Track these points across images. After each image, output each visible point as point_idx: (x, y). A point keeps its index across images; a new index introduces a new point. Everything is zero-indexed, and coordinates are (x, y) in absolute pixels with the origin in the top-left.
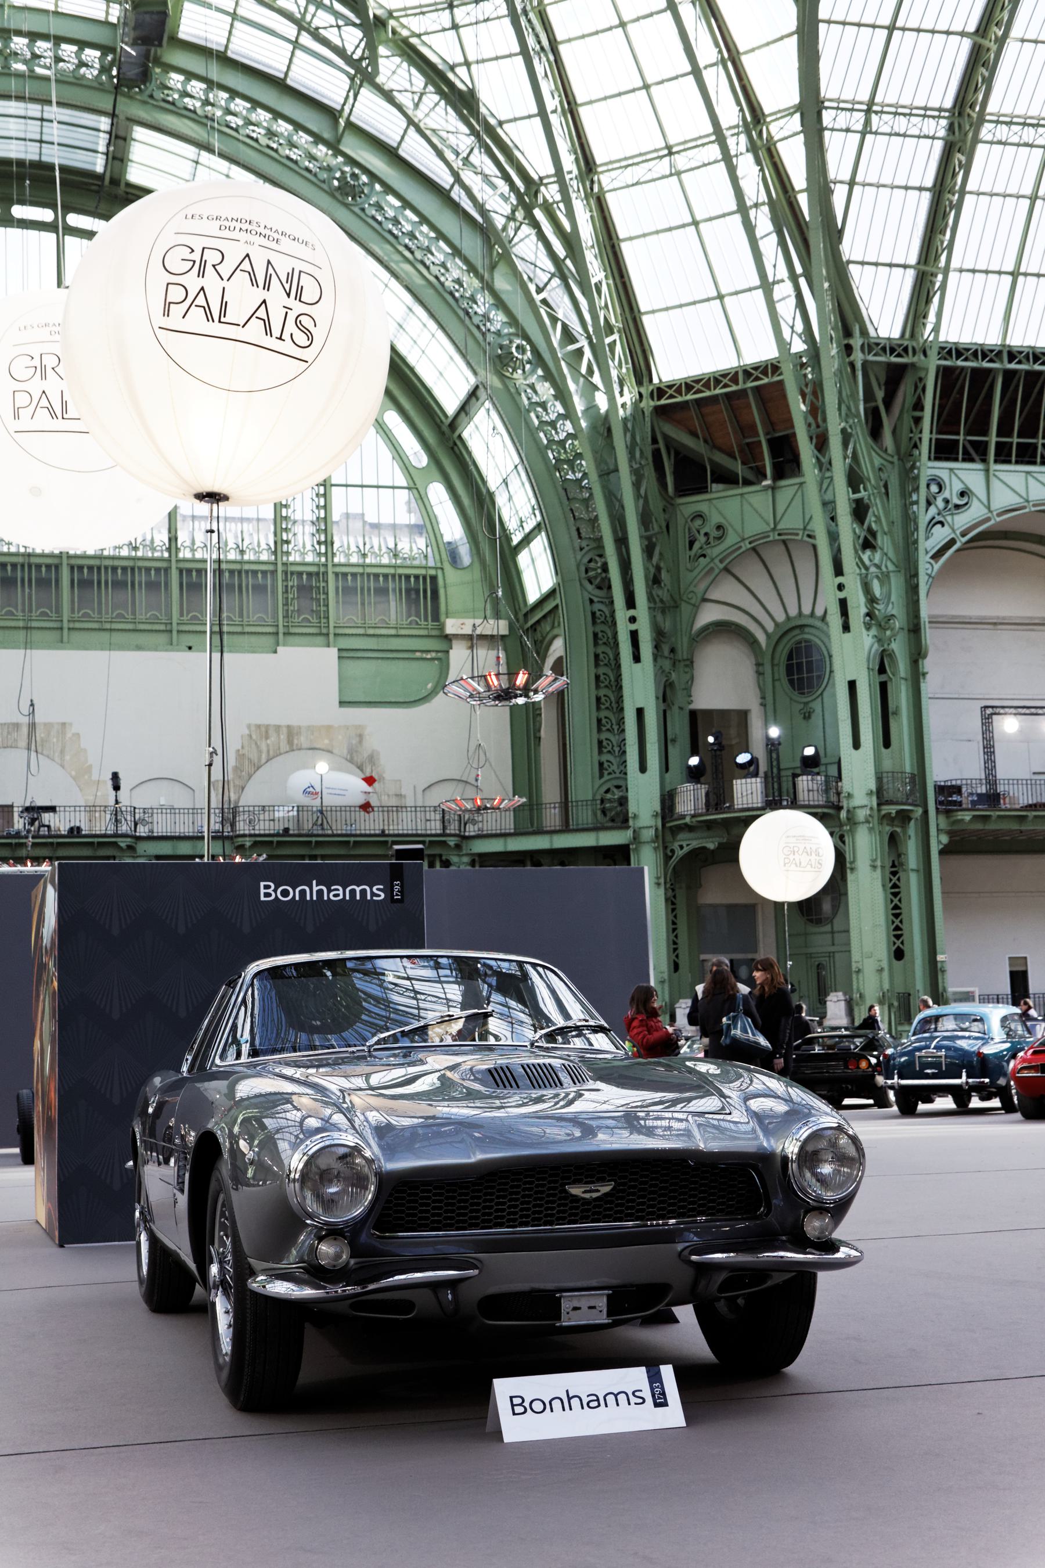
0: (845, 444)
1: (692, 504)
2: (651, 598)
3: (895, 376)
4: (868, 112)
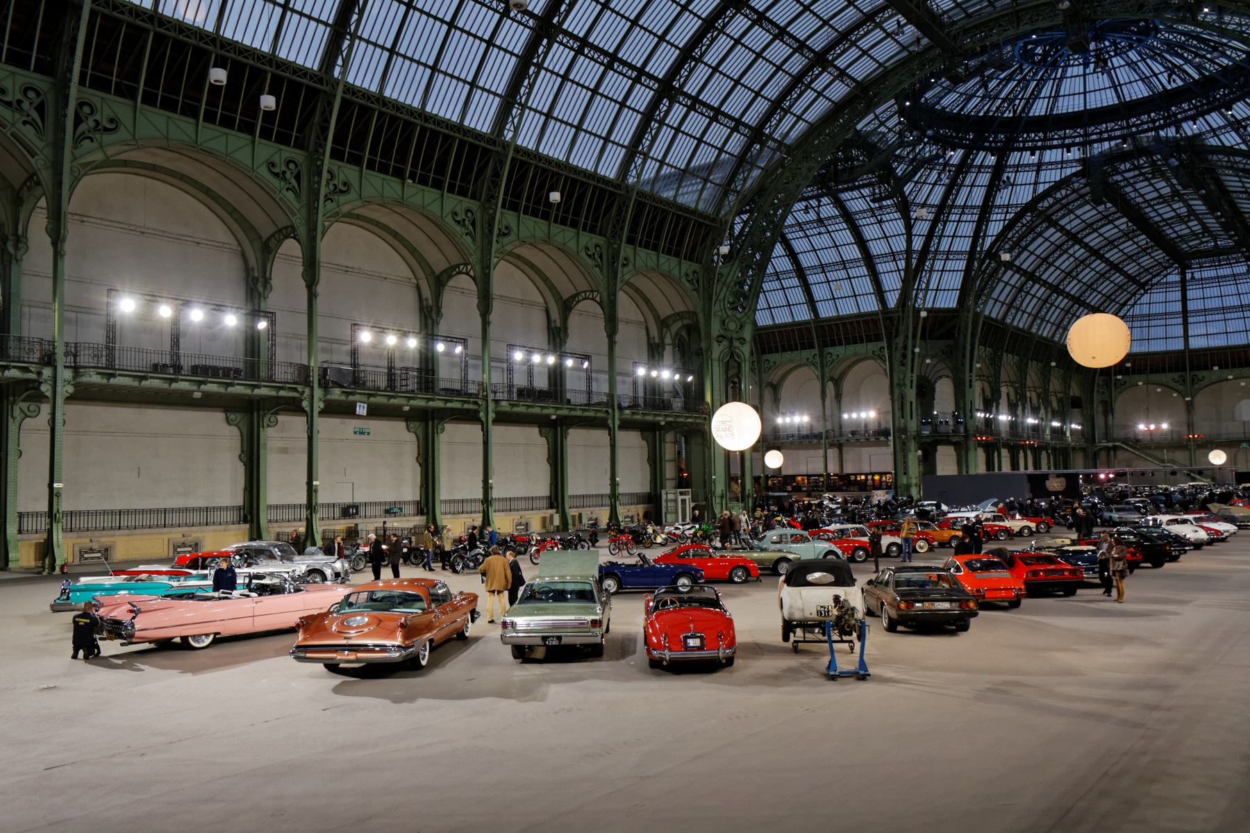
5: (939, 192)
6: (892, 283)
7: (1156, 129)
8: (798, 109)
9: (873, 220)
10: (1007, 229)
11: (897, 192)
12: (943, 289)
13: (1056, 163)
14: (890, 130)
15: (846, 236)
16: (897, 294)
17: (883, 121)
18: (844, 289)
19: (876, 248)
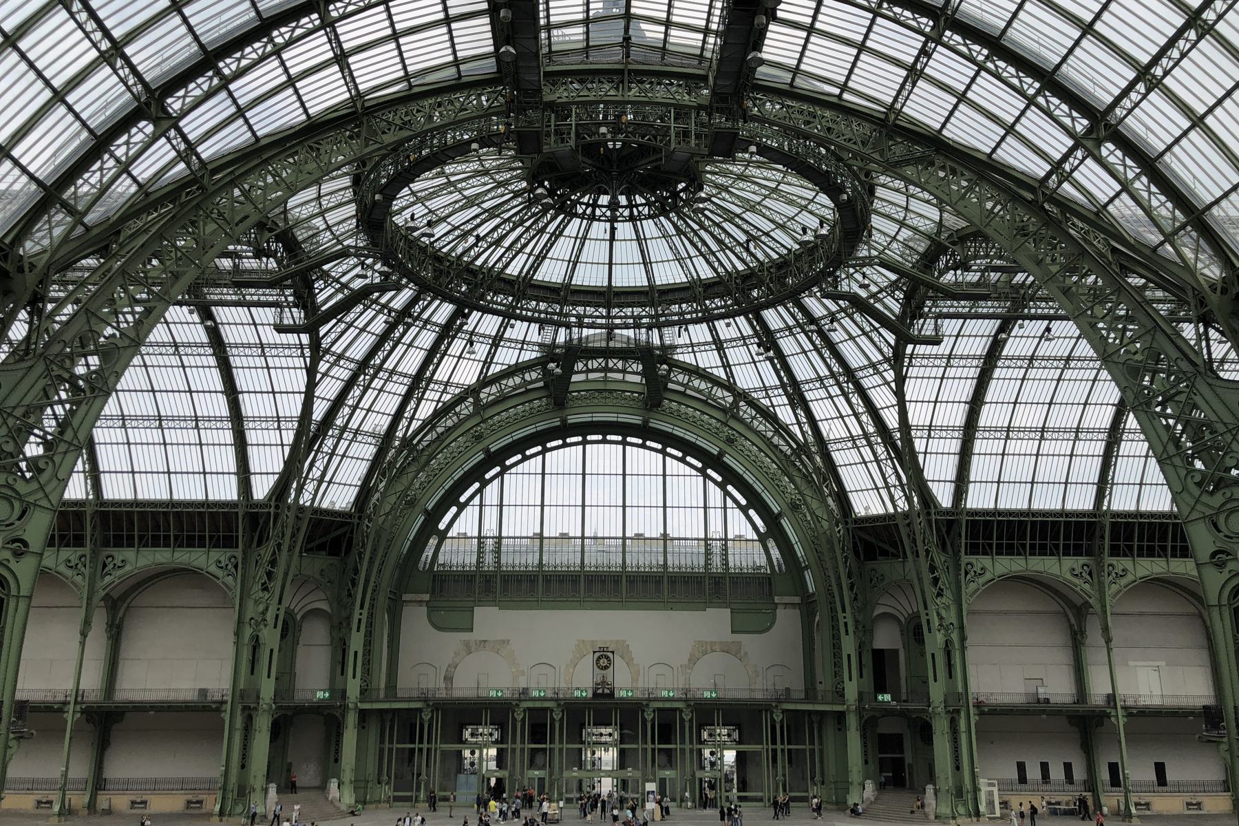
0: (927, 556)
1: (870, 565)
2: (853, 608)
3: (950, 524)
4: (930, 430)
5: (366, 342)
6: (268, 463)
7: (637, 326)
8: (245, 89)
9: (260, 362)
10: (438, 414)
11: (311, 328)
12: (339, 485)
13: (517, 341)
14: (329, 228)
15: (214, 379)
16: (271, 481)
17: (325, 208)
18: (185, 459)
19: (249, 406)
